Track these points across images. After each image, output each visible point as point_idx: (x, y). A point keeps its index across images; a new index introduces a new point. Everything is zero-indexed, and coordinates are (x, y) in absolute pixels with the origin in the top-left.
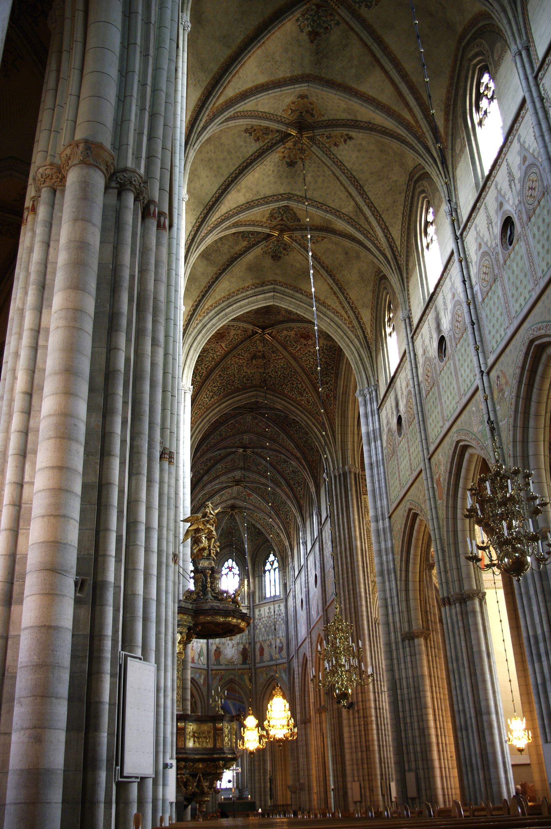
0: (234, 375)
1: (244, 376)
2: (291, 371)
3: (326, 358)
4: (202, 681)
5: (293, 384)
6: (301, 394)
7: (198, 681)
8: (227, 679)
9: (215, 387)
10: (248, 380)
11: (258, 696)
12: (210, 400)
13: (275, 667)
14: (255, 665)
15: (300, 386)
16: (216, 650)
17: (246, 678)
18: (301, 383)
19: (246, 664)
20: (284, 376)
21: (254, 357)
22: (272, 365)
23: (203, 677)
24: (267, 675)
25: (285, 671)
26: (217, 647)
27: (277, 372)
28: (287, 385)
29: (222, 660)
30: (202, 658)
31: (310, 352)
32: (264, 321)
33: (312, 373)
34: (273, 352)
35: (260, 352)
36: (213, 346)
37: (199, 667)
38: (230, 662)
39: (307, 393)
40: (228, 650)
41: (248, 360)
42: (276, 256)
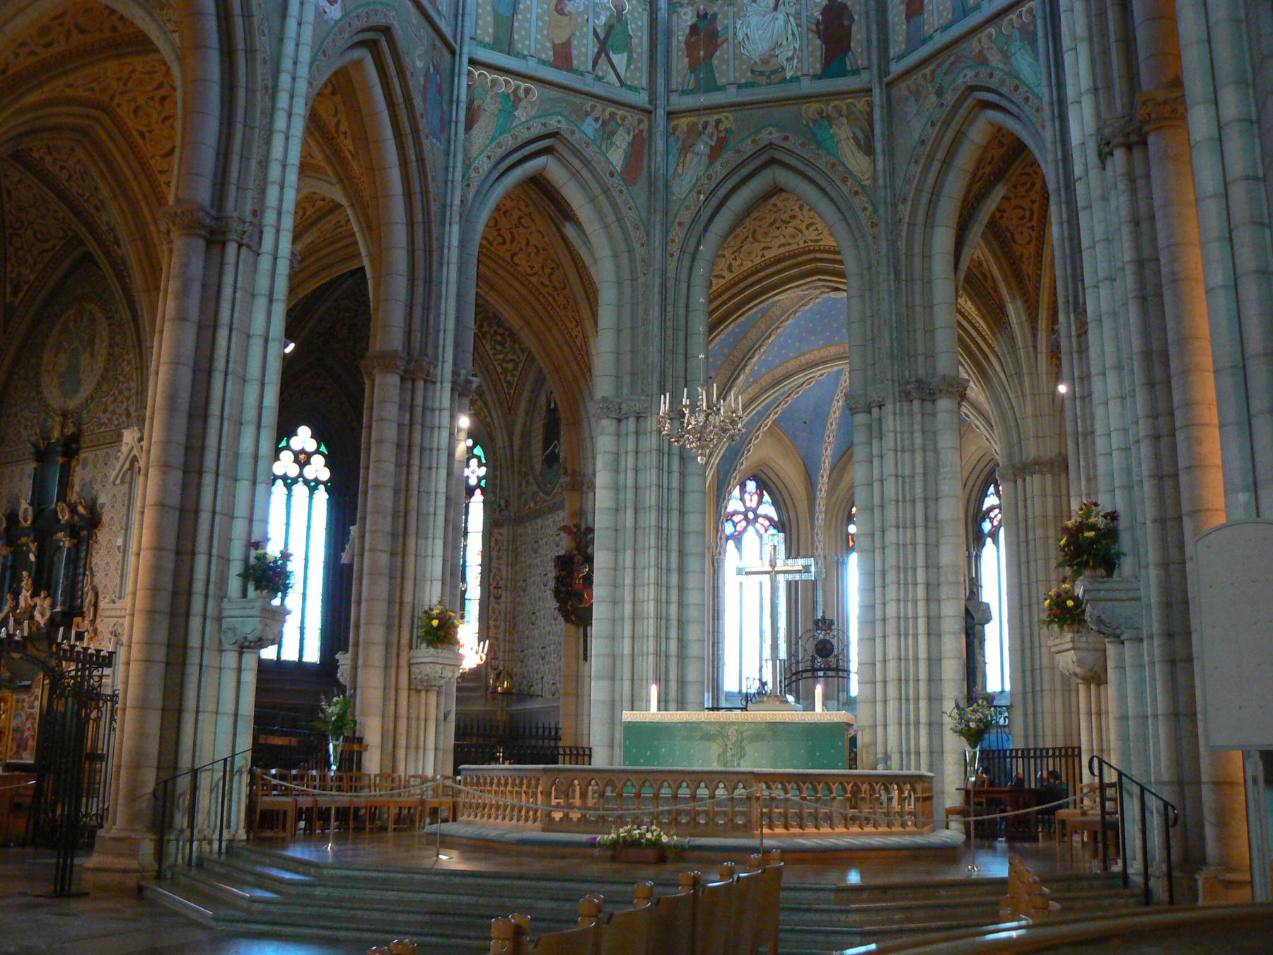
4: (617, 158)
7: (589, 152)
8: (748, 147)
11: (905, 211)
13: (974, 44)
14: (883, 71)
16: (694, 29)
17: (843, 133)
19: (843, 74)
23: (622, 140)
24: (940, 93)
25: (1030, 38)
26: (702, 16)
29: (726, 67)
30: (619, 59)
37: (598, 89)
38: (767, 71)
40: (754, 20)
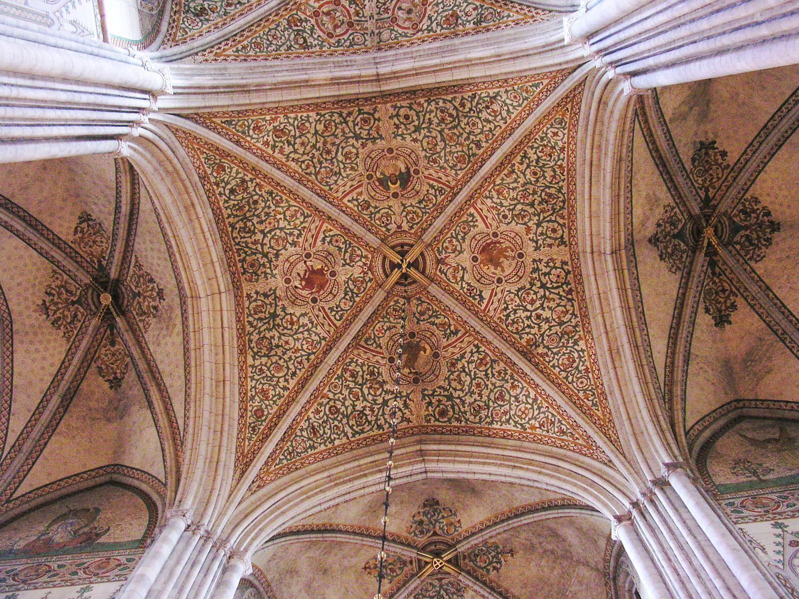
0: (443, 140)
1: (417, 129)
2: (316, 174)
3: (255, 243)
5: (303, 144)
6: (279, 132)
9: (489, 122)
10: (407, 117)
12: (498, 94)
15: (288, 149)
18: (288, 157)
20: (329, 152)
21: (405, 179)
22: (361, 168)
27: (347, 156)
28: (316, 132)
31: (294, 244)
32: (408, 299)
33: (271, 193)
34: (366, 205)
35: (395, 195)
36: (503, 227)
39: (266, 143)
41: (417, 172)
42: (431, 506)
